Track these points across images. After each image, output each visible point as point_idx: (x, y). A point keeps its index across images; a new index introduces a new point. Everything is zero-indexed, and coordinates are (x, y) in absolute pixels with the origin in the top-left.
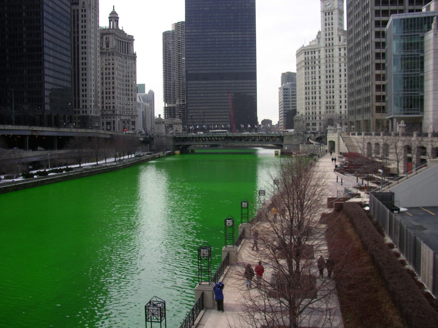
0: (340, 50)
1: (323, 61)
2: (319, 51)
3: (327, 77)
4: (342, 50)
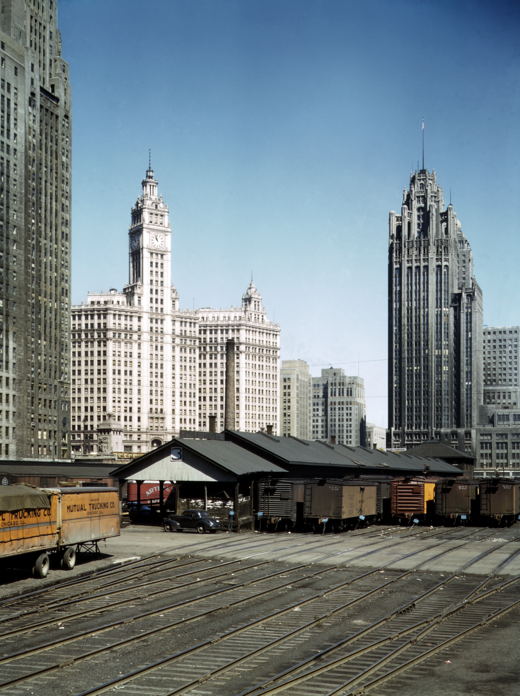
0: (174, 325)
1: (146, 337)
2: (139, 318)
3: (151, 367)
4: (178, 324)
